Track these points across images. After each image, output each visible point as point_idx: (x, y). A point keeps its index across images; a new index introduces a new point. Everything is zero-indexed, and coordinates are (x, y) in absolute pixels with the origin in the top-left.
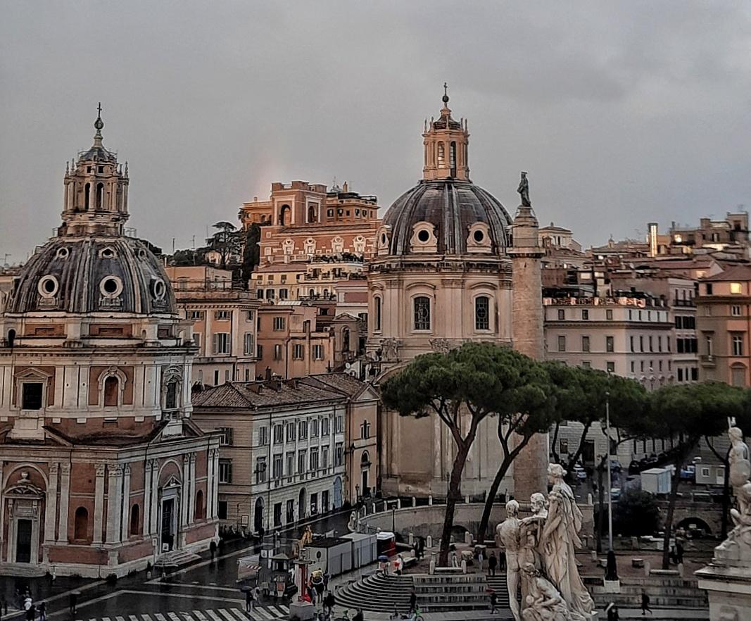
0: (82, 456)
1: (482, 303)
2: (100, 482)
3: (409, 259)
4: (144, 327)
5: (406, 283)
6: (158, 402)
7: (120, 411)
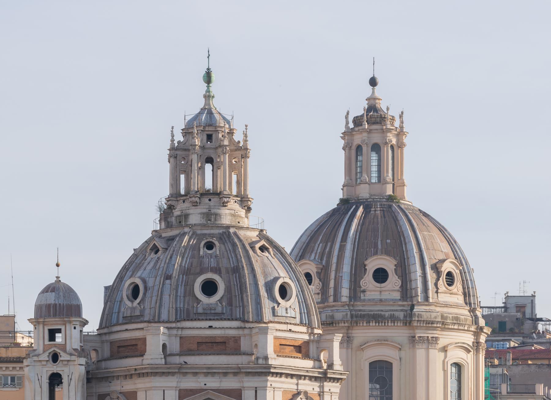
3: (359, 306)
5: (356, 342)
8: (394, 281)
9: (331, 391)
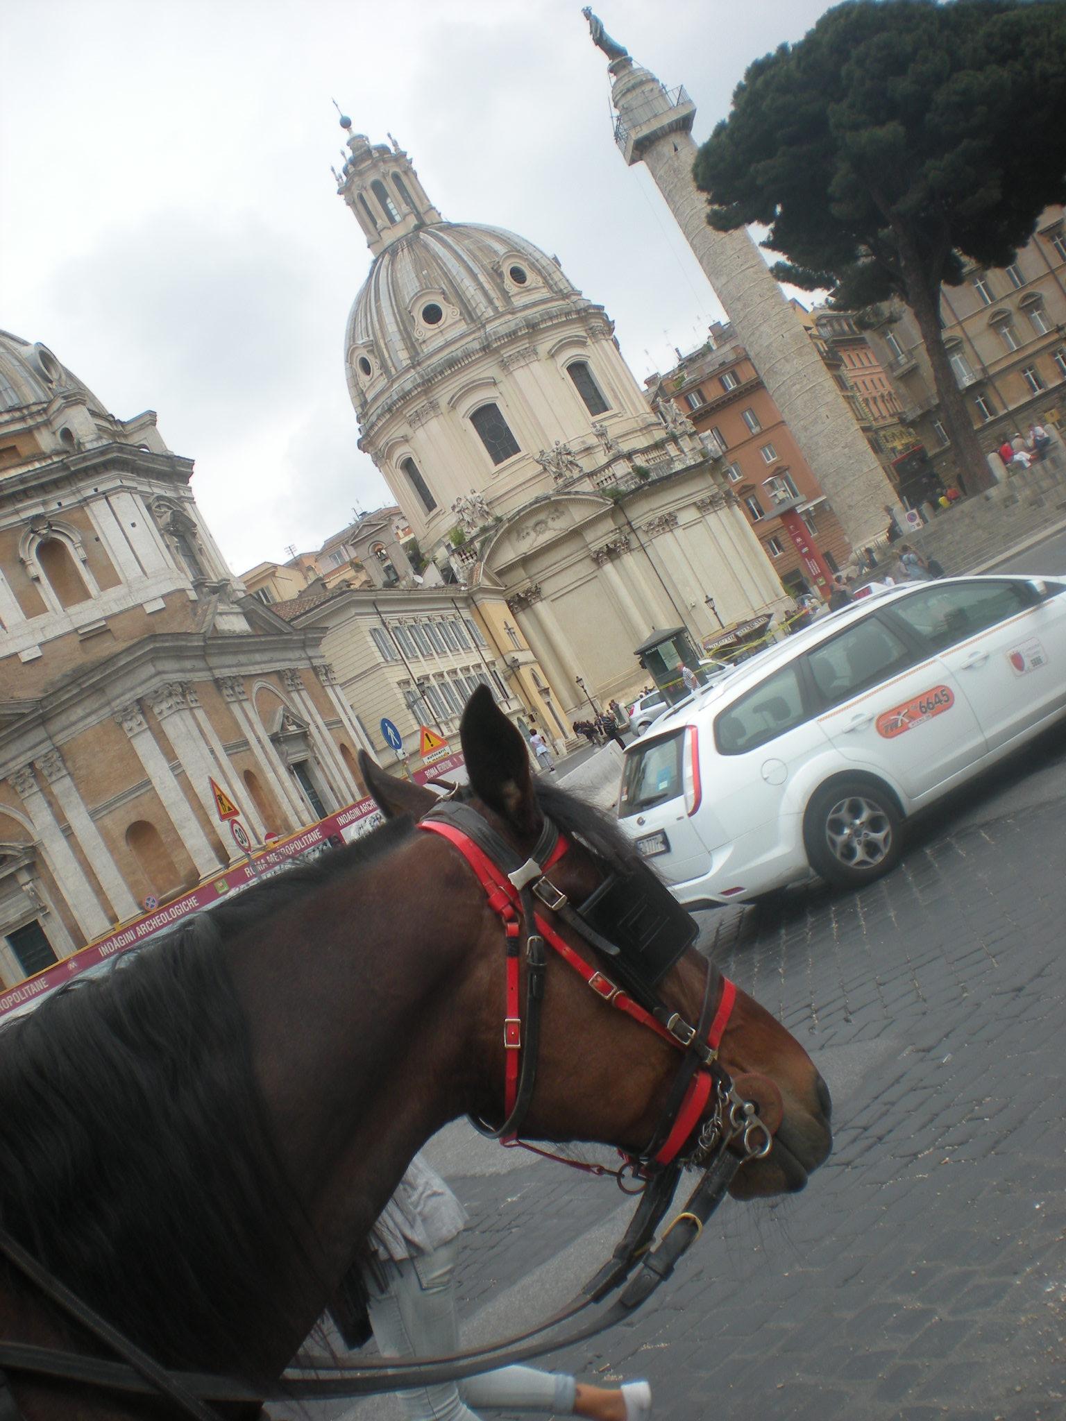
0: (73, 718)
1: (578, 370)
2: (145, 746)
4: (59, 424)
5: (443, 402)
6: (171, 563)
7: (99, 606)
8: (450, 313)
9: (100, 490)
